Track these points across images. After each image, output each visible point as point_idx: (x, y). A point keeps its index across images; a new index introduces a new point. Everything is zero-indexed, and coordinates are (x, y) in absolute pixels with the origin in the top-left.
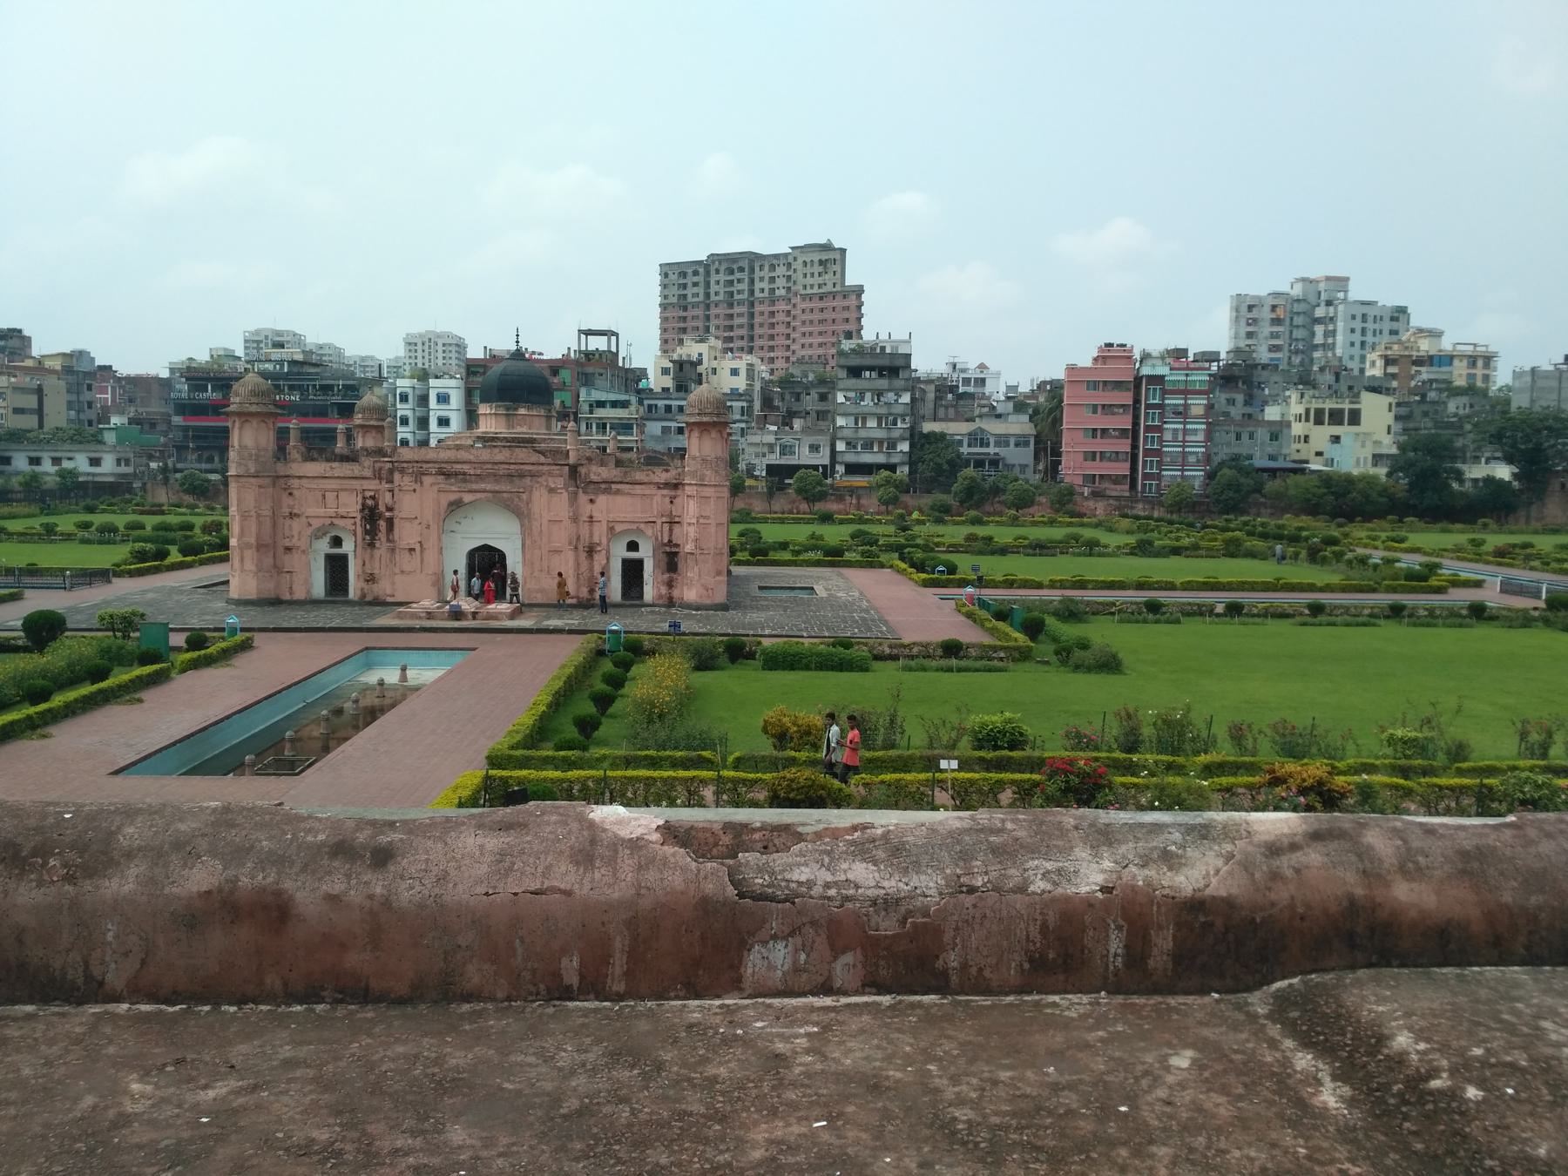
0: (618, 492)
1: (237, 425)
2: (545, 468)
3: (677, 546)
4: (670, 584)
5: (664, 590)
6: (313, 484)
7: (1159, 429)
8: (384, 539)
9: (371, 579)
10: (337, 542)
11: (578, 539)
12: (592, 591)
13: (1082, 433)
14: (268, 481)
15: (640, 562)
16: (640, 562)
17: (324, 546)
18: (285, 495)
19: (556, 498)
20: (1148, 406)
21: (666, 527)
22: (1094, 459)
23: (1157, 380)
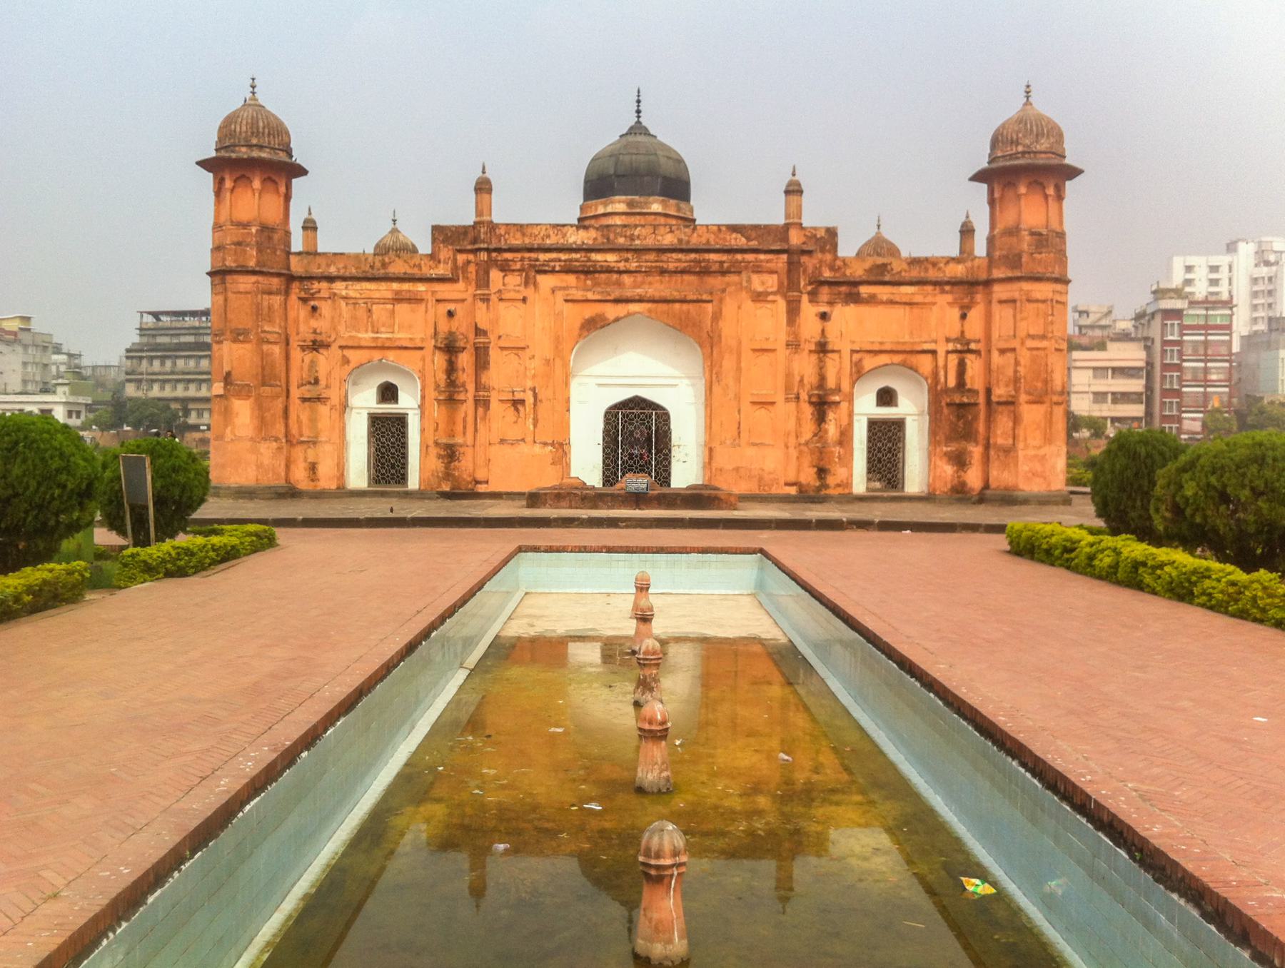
0: (872, 300)
1: (228, 184)
2: (750, 257)
3: (973, 392)
4: (960, 461)
5: (948, 470)
6: (354, 290)
7: (1178, 368)
8: (471, 387)
9: (450, 454)
10: (388, 393)
11: (801, 381)
12: (822, 472)
13: (1090, 372)
14: (275, 281)
15: (899, 424)
16: (899, 424)
17: (365, 400)
18: (303, 312)
19: (763, 311)
20: (1165, 343)
21: (953, 360)
22: (1105, 401)
23: (1177, 314)
